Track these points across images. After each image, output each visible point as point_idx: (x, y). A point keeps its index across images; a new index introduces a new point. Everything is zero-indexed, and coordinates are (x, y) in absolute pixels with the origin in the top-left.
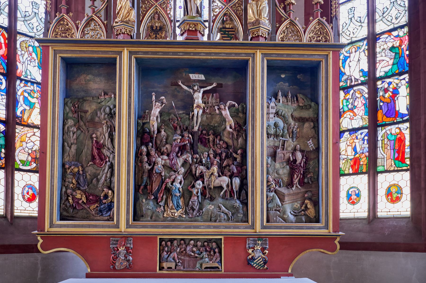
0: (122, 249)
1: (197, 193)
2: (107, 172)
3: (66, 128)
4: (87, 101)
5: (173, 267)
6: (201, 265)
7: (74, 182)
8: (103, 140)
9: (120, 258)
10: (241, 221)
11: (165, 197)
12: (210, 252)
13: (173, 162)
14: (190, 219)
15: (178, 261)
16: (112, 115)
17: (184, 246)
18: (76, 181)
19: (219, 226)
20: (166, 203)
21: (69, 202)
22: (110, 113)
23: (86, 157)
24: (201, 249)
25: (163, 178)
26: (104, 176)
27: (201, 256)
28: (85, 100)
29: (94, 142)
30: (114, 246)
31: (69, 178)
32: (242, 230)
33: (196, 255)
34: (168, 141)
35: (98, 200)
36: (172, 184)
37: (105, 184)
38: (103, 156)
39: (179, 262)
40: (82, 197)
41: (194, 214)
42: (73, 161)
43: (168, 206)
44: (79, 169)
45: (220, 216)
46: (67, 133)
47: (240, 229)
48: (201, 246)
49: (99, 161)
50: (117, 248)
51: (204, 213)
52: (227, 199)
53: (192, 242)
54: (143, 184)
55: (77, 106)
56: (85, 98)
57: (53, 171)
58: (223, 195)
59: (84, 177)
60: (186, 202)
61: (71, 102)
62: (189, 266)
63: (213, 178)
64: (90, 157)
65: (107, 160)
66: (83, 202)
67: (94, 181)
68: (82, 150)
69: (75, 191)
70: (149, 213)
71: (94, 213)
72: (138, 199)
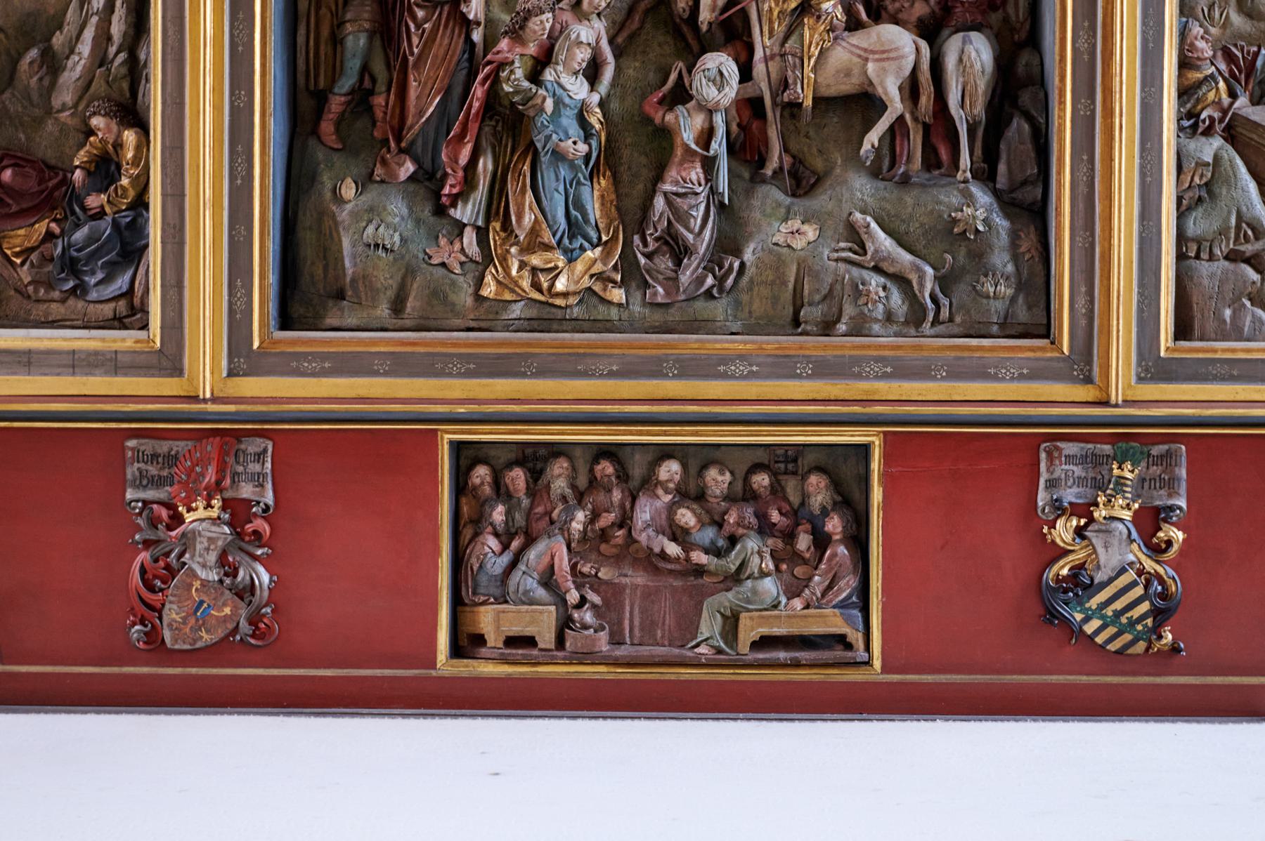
1: (706, 137)
5: (547, 638)
6: (731, 623)
10: (1002, 325)
11: (486, 165)
14: (657, 317)
15: (573, 597)
17: (617, 495)
19: (856, 361)
20: (497, 207)
24: (732, 518)
25: (477, 36)
26: (89, 34)
27: (732, 562)
32: (1001, 387)
33: (699, 557)
36: (535, 76)
37: (98, 86)
39: (583, 600)
41: (685, 278)
43: (506, 226)
45: (857, 293)
47: (995, 378)
48: (730, 498)
51: (751, 271)
52: (905, 181)
53: (670, 470)
54: (347, 83)
58: (878, 150)
60: (633, 203)
62: (649, 627)
63: (812, 34)
70: (385, 276)
71: (25, 274)
72: (313, 178)
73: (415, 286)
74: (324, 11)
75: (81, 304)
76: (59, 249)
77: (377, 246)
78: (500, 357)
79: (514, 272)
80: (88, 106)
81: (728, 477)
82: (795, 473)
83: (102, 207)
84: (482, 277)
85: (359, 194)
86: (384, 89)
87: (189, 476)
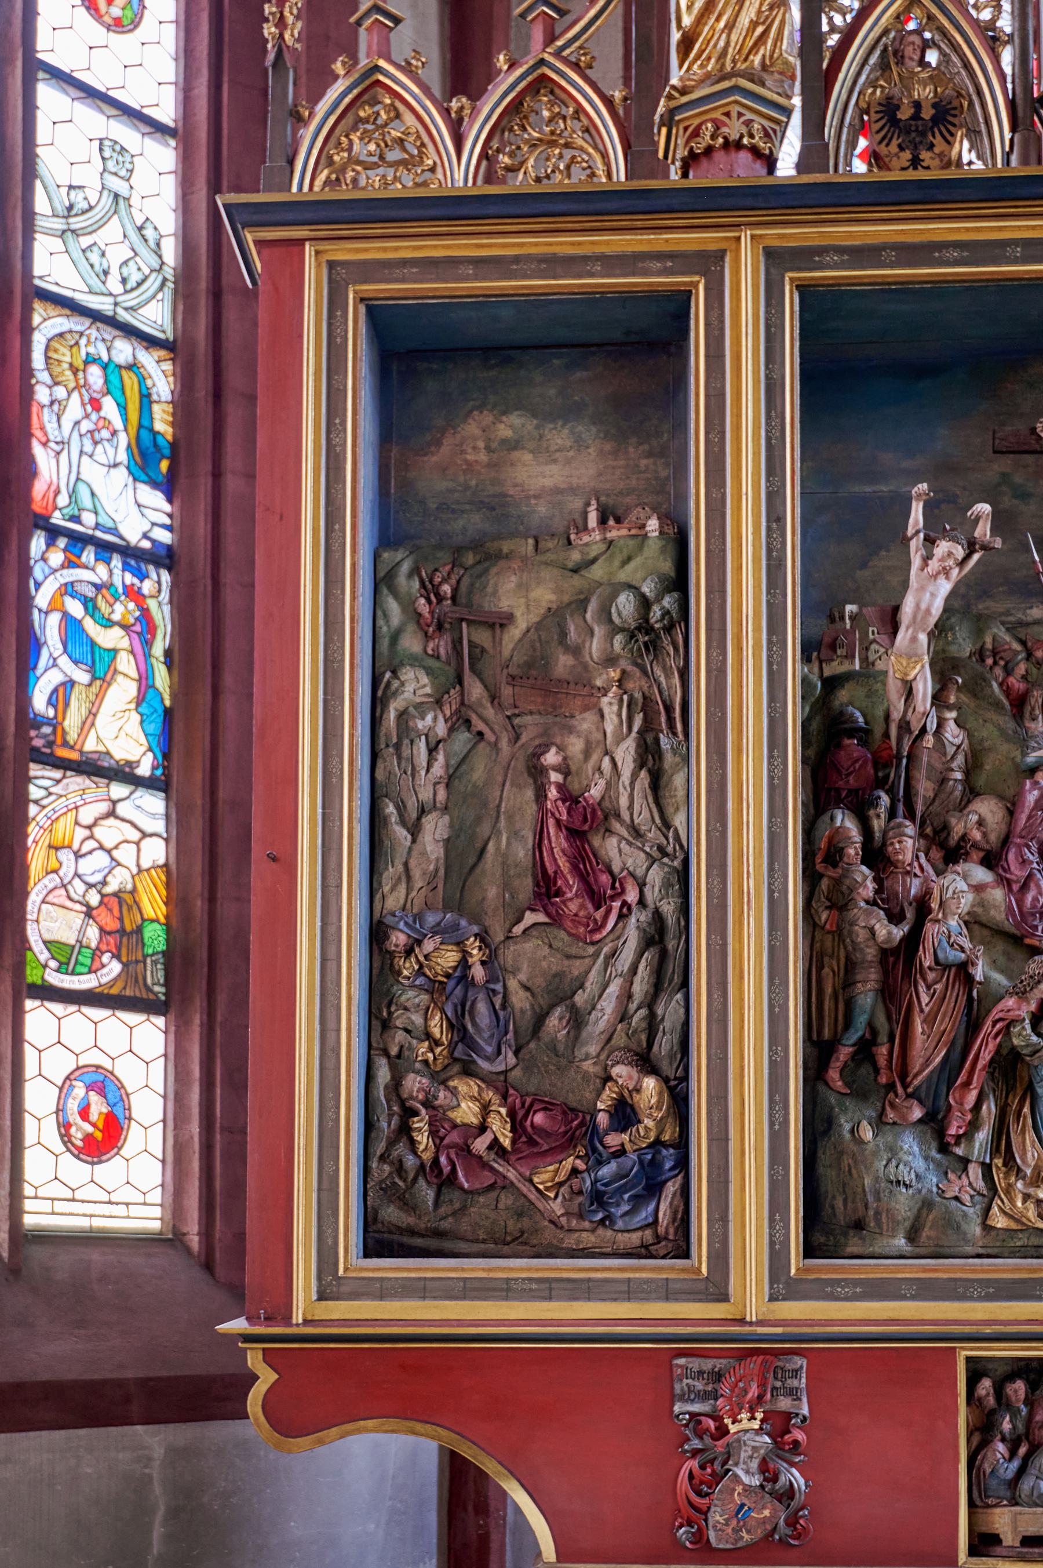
0: (745, 1424)
2: (634, 970)
3: (392, 715)
4: (502, 563)
7: (436, 1032)
8: (602, 783)
9: (736, 1478)
11: (990, 1109)
13: (1029, 898)
16: (657, 635)
18: (451, 1026)
20: (1002, 1143)
21: (413, 1143)
22: (644, 626)
23: (506, 886)
26: (614, 988)
28: (499, 556)
29: (553, 793)
30: (696, 1408)
31: (412, 1004)
34: (981, 781)
35: (577, 1132)
38: (605, 879)
40: (485, 1109)
42: (428, 906)
43: (1009, 1160)
44: (465, 954)
46: (398, 746)
49: (582, 906)
50: (717, 1418)
54: (853, 1037)
55: (446, 589)
56: (492, 546)
57: (331, 966)
59: (498, 1001)
61: (415, 571)
64: (526, 886)
65: (632, 896)
66: (495, 1145)
67: (555, 1023)
68: (479, 845)
69: (444, 1083)
71: (557, 1207)
72: (830, 1123)
73: (931, 1217)
74: (826, 970)
75: (609, 1233)
76: (588, 1183)
77: (898, 1182)
78: (1023, 1281)
79: (1019, 1204)
80: (608, 1057)
83: (622, 1145)
84: (989, 1208)
85: (875, 1136)
86: (885, 1040)
87: (732, 1391)
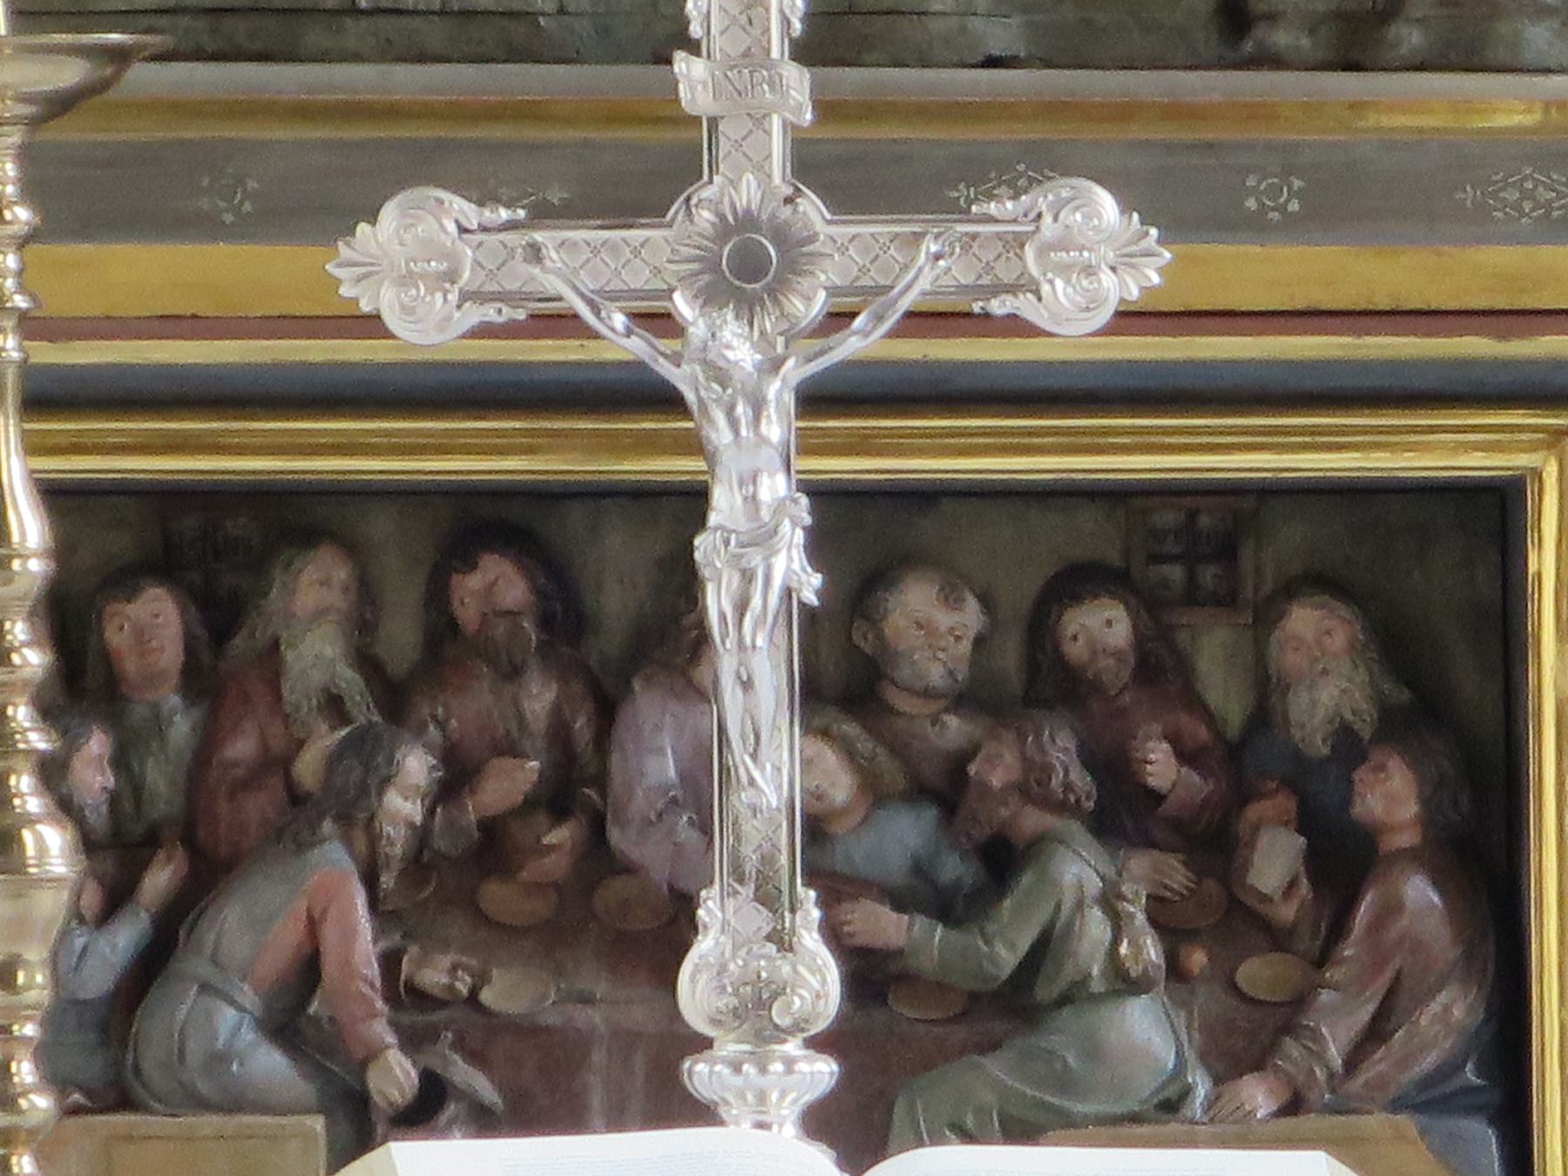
12: (1213, 843)
48: (970, 697)
81: (971, 616)
82: (1227, 600)
